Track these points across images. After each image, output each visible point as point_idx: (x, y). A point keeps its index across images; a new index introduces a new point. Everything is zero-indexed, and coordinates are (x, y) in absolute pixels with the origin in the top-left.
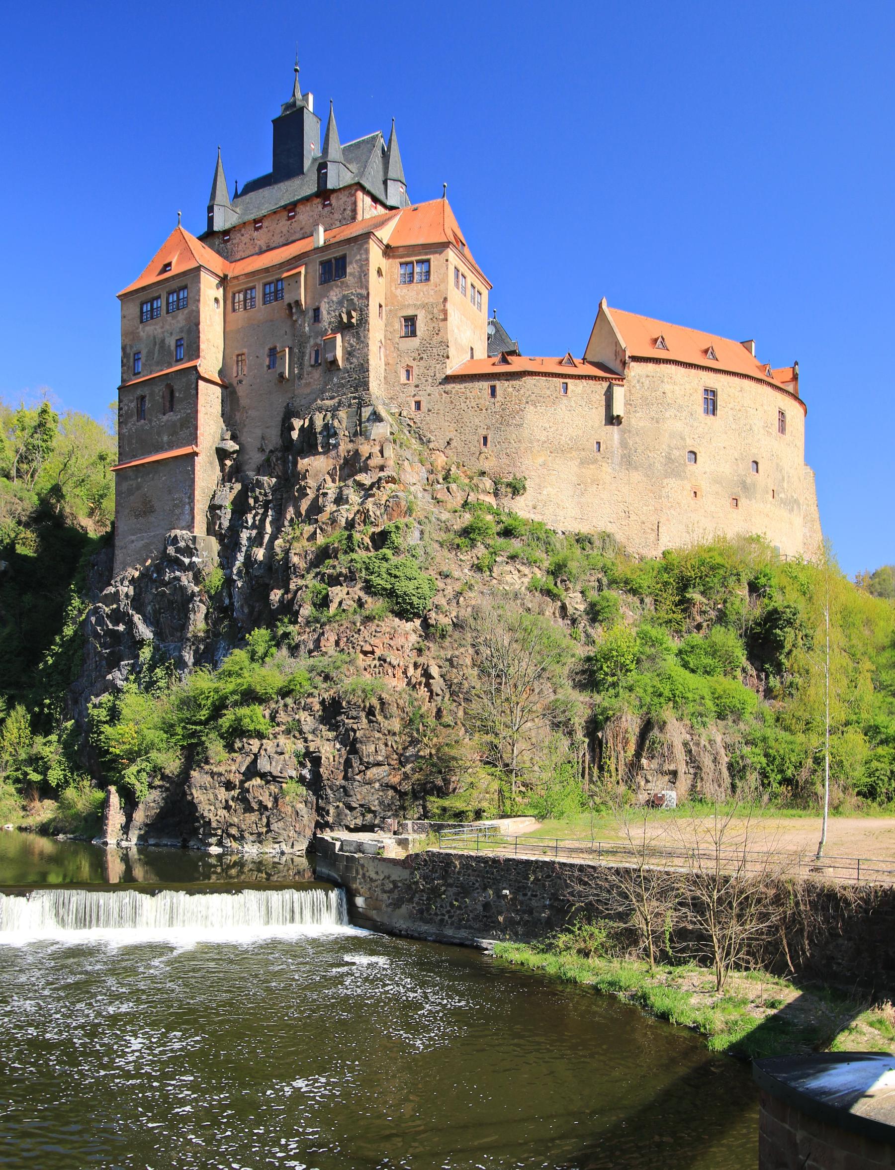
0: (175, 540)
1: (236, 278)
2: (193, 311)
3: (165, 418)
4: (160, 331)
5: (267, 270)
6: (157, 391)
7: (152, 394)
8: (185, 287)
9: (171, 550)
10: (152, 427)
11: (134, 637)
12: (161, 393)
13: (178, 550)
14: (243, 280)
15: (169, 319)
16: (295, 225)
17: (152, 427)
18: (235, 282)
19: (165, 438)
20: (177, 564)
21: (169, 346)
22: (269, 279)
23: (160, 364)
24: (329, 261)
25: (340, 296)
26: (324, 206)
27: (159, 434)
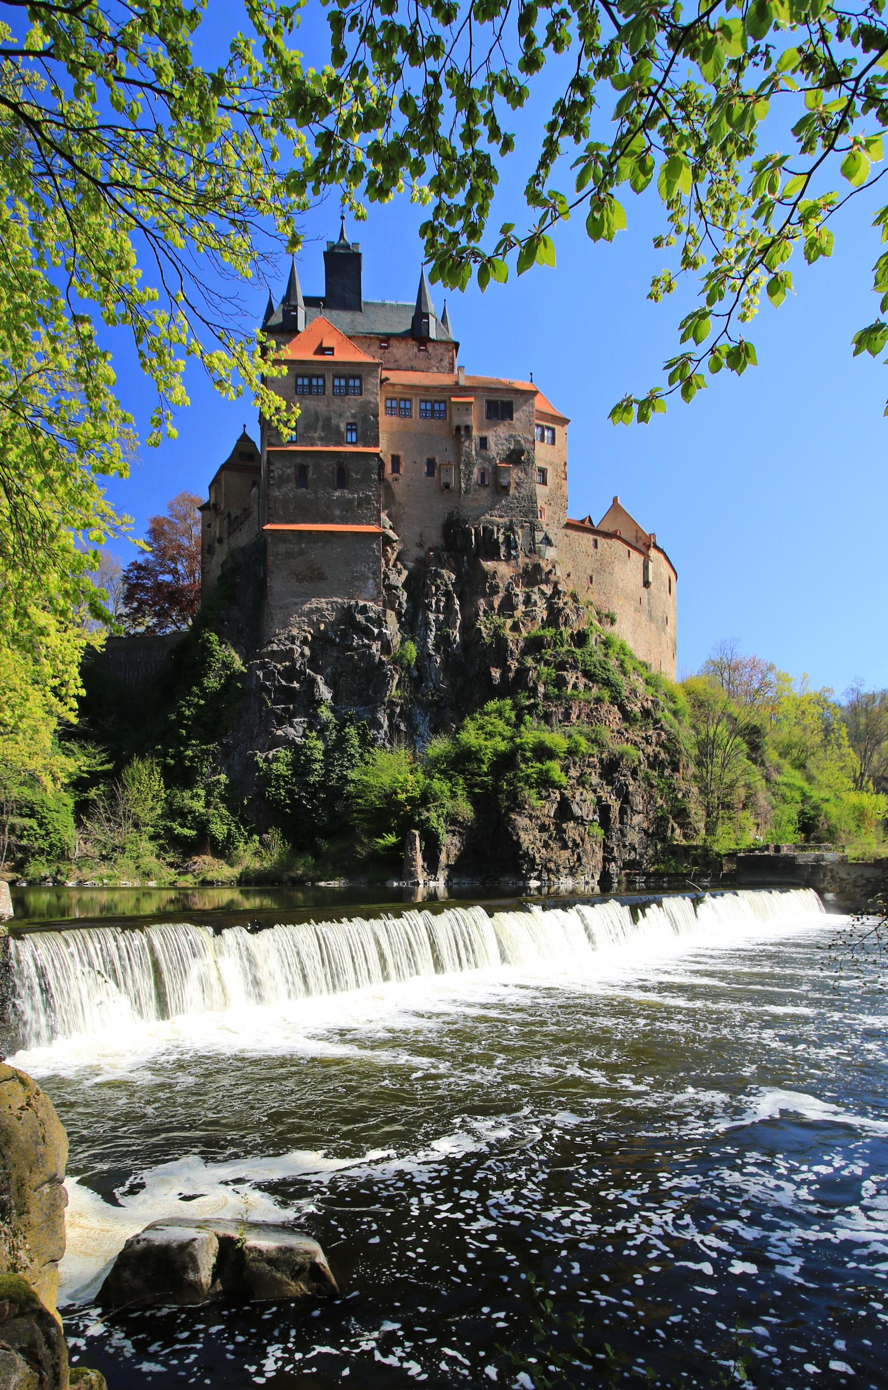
0: (364, 610)
1: (393, 385)
2: (370, 402)
4: (324, 409)
5: (427, 388)
8: (359, 377)
9: (360, 618)
11: (314, 695)
13: (368, 619)
14: (398, 389)
15: (337, 401)
16: (388, 355)
18: (390, 388)
20: (367, 633)
21: (338, 427)
22: (427, 398)
23: (325, 441)
24: (495, 402)
25: (507, 435)
26: (420, 350)
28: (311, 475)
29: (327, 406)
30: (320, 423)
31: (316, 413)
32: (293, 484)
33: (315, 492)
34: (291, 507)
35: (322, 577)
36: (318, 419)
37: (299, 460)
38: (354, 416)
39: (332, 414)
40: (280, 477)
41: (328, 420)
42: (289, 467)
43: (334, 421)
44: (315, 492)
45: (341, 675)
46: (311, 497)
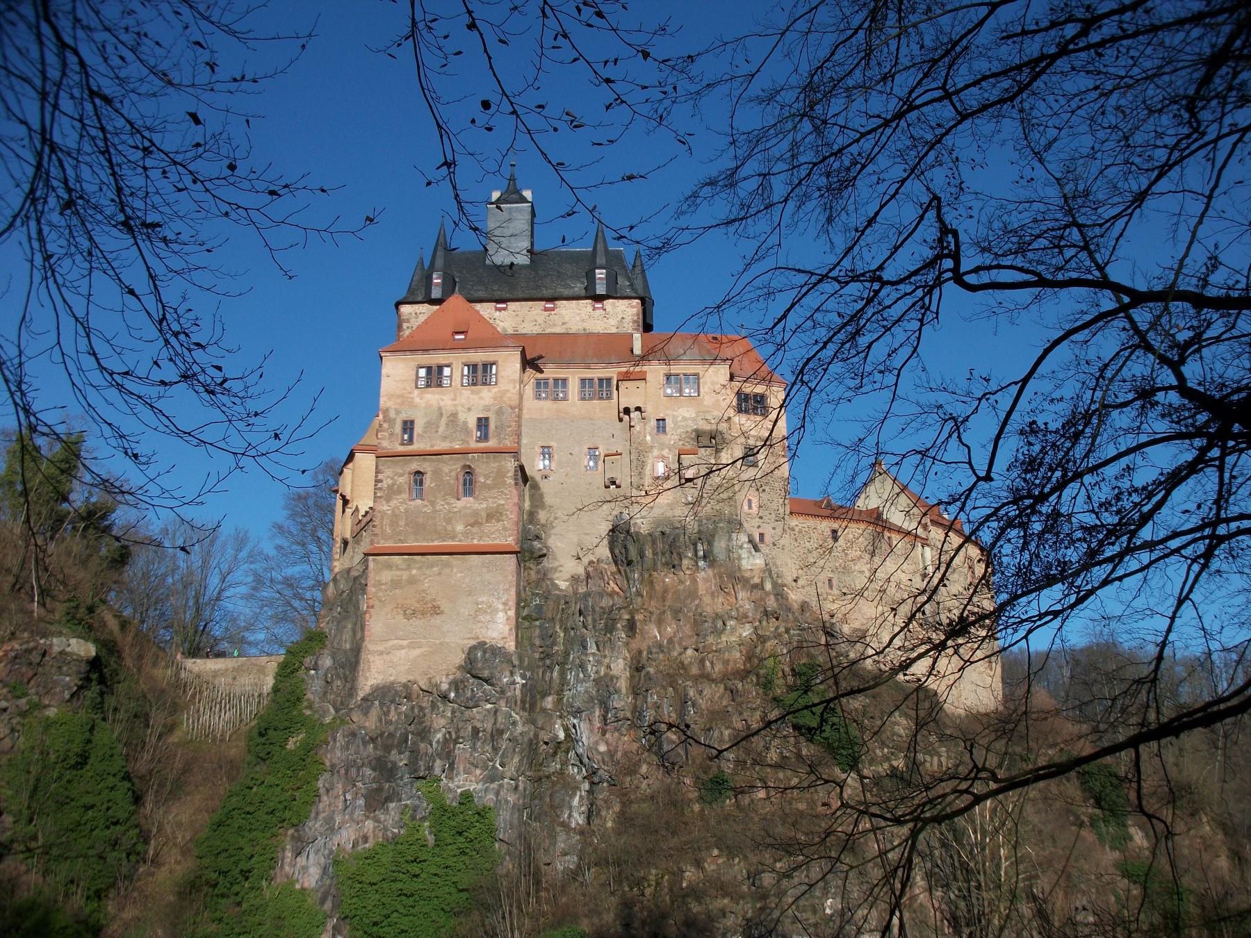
3: (459, 504)
6: (446, 469)
7: (436, 473)
10: (435, 511)
12: (453, 474)
15: (467, 392)
17: (435, 511)
19: (460, 528)
21: (465, 423)
27: (449, 521)
28: (428, 481)
29: (454, 400)
30: (444, 420)
31: (440, 408)
32: (405, 496)
33: (433, 503)
34: (402, 523)
35: (436, 610)
36: (441, 415)
37: (415, 465)
38: (487, 409)
39: (459, 408)
40: (390, 487)
41: (454, 416)
42: (401, 475)
43: (462, 417)
44: (433, 503)
45: (456, 742)
46: (428, 510)
